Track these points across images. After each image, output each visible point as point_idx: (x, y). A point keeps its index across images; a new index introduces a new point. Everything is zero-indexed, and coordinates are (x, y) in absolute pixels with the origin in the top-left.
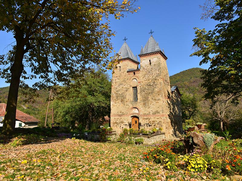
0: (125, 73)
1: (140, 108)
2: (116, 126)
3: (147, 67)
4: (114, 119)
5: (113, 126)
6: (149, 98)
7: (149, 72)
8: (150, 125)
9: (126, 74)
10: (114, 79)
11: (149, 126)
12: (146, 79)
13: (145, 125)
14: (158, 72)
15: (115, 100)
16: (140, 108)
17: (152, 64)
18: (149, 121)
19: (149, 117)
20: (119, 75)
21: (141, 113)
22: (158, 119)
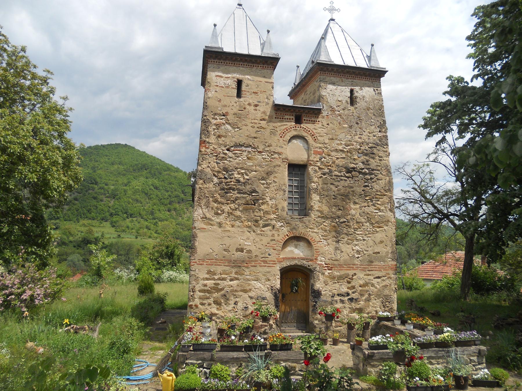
0: (261, 108)
1: (318, 239)
2: (217, 303)
3: (342, 107)
4: (209, 272)
5: (203, 304)
6: (353, 212)
7: (351, 127)
8: (354, 296)
9: (264, 112)
10: (214, 121)
11: (351, 300)
12: (340, 148)
13: (337, 298)
14: (380, 134)
15: (216, 201)
16: (318, 239)
17: (361, 104)
18: (350, 285)
19: (351, 272)
20: (235, 110)
21: (321, 260)
22: (379, 277)
